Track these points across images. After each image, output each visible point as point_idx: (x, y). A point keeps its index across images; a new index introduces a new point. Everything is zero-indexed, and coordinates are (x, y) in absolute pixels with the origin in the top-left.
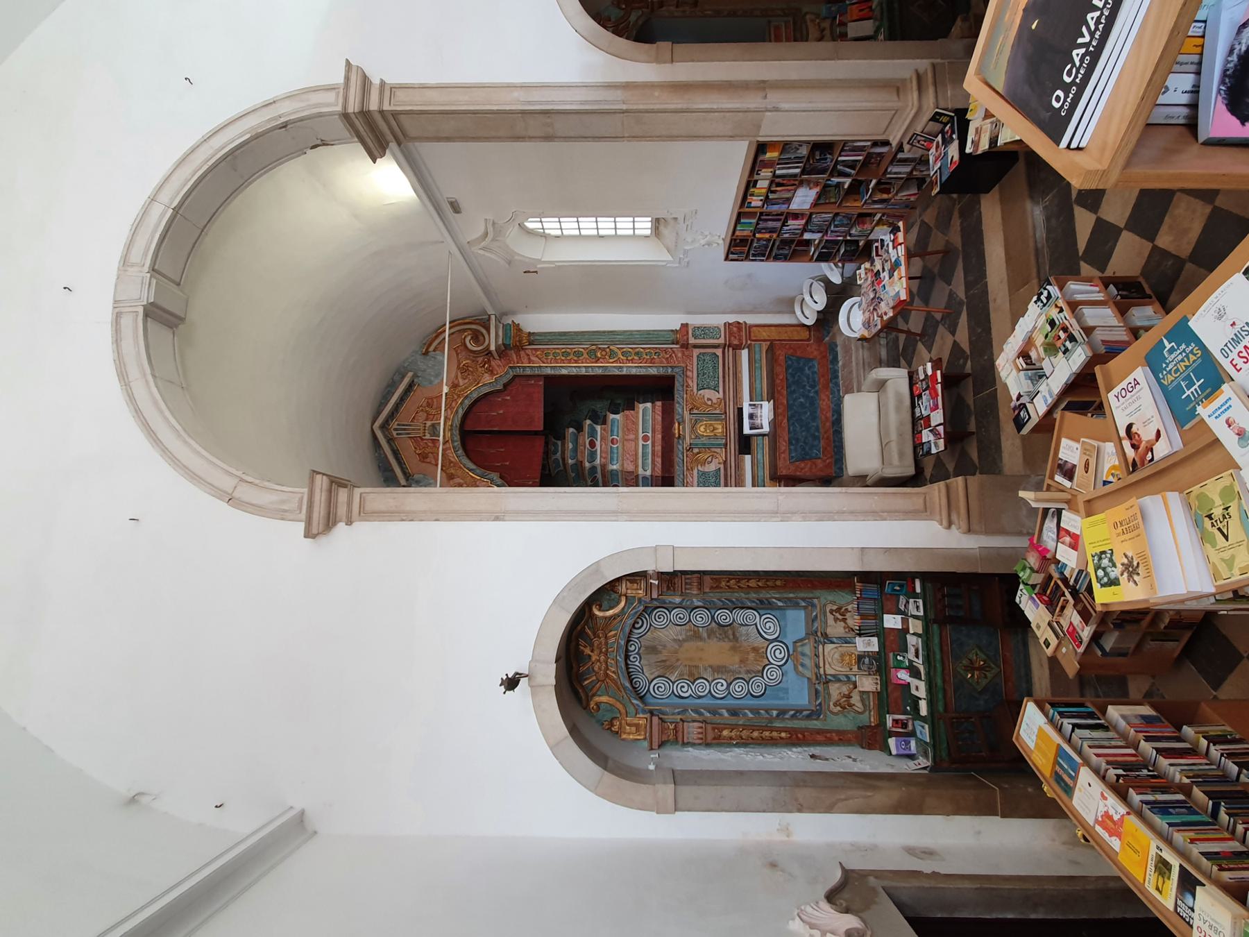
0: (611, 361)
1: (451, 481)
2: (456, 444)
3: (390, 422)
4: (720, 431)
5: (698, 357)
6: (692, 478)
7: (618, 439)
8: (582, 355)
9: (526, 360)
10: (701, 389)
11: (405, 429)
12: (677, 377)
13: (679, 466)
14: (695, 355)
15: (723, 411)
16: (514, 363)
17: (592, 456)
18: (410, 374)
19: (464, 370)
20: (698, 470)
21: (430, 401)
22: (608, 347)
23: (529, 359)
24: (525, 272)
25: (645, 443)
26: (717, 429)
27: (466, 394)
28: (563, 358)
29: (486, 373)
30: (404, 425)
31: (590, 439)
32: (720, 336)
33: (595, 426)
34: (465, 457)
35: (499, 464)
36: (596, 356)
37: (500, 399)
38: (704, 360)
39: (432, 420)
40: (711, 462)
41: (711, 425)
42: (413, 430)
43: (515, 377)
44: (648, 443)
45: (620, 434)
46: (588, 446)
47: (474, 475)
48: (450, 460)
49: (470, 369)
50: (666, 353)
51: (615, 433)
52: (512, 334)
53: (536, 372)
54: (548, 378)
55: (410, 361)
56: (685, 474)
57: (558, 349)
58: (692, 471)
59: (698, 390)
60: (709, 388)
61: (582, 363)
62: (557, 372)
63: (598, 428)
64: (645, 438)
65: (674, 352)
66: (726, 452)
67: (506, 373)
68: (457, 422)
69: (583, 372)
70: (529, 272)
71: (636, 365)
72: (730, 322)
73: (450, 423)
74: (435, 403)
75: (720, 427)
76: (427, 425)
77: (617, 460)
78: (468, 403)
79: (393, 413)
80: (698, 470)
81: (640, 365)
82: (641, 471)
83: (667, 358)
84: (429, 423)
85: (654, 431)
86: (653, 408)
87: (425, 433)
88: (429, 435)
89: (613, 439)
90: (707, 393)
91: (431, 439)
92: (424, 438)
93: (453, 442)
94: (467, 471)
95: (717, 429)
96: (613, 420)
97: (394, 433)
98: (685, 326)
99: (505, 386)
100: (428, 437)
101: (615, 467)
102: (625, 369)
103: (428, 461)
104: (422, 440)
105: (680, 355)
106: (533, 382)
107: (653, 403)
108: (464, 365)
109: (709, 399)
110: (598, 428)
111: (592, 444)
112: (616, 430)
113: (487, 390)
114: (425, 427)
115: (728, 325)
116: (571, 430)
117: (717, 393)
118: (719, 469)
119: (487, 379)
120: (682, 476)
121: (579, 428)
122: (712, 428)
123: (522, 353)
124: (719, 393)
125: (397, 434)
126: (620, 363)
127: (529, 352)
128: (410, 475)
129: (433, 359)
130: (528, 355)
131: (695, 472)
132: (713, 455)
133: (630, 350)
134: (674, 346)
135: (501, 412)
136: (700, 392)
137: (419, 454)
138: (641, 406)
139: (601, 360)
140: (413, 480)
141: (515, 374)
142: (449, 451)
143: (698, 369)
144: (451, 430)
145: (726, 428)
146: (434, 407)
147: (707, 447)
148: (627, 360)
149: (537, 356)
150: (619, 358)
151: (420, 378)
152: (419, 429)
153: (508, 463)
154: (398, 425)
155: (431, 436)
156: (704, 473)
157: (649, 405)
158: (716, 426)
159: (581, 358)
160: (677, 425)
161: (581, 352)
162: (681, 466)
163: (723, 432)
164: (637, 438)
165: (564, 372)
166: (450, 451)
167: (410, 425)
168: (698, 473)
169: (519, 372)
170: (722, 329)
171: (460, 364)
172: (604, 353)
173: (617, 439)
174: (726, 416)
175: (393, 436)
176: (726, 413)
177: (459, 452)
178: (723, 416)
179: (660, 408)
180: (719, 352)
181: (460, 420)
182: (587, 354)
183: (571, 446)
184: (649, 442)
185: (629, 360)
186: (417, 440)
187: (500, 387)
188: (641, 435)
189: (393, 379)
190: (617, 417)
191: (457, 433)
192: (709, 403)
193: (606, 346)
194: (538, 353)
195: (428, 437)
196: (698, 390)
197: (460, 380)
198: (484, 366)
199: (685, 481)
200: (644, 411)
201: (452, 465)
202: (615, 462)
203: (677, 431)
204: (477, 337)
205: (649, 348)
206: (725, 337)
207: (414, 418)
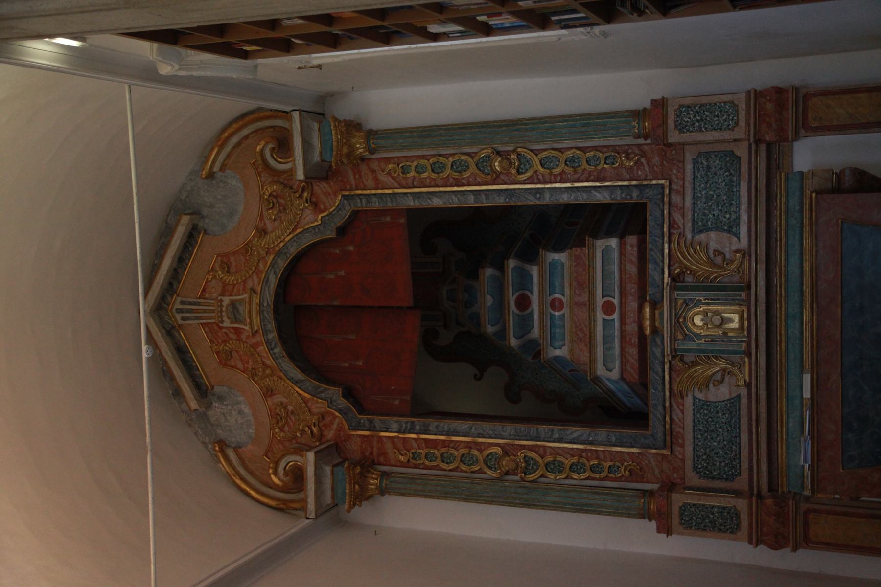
0: (522, 177)
1: (269, 399)
2: (270, 336)
3: (169, 298)
4: (735, 325)
5: (695, 161)
6: (683, 412)
7: (564, 300)
8: (468, 167)
9: (370, 182)
10: (701, 232)
11: (192, 311)
12: (650, 207)
13: (656, 389)
14: (689, 157)
15: (746, 277)
16: (351, 190)
17: (525, 324)
18: (185, 219)
19: (273, 202)
20: (694, 398)
21: (225, 260)
22: (514, 151)
23: (376, 179)
24: (299, 68)
25: (606, 317)
26: (731, 320)
27: (277, 249)
28: (434, 176)
29: (306, 208)
30: (191, 304)
31: (517, 294)
32: (737, 124)
33: (528, 267)
34: (287, 359)
35: (347, 365)
36: (493, 171)
37: (337, 252)
38: (709, 168)
39: (231, 295)
40: (721, 381)
41: (717, 313)
42: (205, 311)
43: (356, 214)
44: (611, 317)
45: (567, 291)
46: (513, 307)
47: (300, 392)
48: (264, 364)
49: (282, 201)
50: (628, 158)
51: (557, 290)
52: (335, 144)
53: (389, 204)
54: (412, 214)
55: (189, 189)
56: (667, 404)
57: (423, 157)
58: (682, 397)
59: (697, 231)
60: (718, 228)
61: (469, 185)
62: (425, 204)
63: (535, 271)
64: (608, 308)
65: (643, 154)
66: (750, 364)
67: (339, 209)
68: (269, 297)
69: (471, 202)
70: (305, 68)
71: (568, 185)
72: (758, 89)
73: (258, 301)
74: (234, 264)
75: (736, 317)
76: (225, 303)
77: (564, 340)
78: (282, 264)
79: (171, 284)
80: (694, 398)
81: (576, 185)
82: (601, 370)
83: (631, 167)
84: (226, 300)
85: (623, 294)
86: (622, 246)
87: (221, 316)
88: (229, 321)
89: (554, 300)
90: (713, 239)
91: (234, 328)
92: (221, 325)
93: (266, 332)
94: (291, 384)
95: (731, 320)
96: (553, 264)
97: (178, 317)
98: (660, 104)
99: (342, 231)
100: (227, 323)
101: (558, 352)
102: (547, 196)
103: (233, 364)
104: (221, 328)
105: (656, 160)
106: (388, 219)
107: (622, 237)
108: (270, 195)
109: (717, 253)
110: (535, 271)
111: (523, 303)
112: (557, 284)
113: (308, 240)
114: (221, 306)
115: (757, 96)
116: (489, 272)
117: (735, 239)
118: (739, 396)
119: (311, 219)
120: (660, 408)
121: (501, 268)
122: (717, 320)
123: (364, 168)
124: (739, 238)
125: (183, 319)
126: (540, 182)
127: (375, 165)
128: (207, 389)
129: (222, 185)
130: (373, 171)
131: (688, 401)
132: (724, 370)
133: (555, 153)
134: (641, 141)
135: (342, 273)
136: (697, 237)
137: (217, 353)
138: (600, 244)
139: (502, 177)
140: (214, 395)
141: (353, 208)
142: (261, 348)
143: (694, 188)
144: (260, 312)
145: (748, 319)
146: (233, 270)
147: (708, 356)
148: (551, 174)
149: (389, 174)
150: (536, 172)
151: (207, 220)
152: (213, 311)
153: (360, 364)
154: (182, 303)
155: (231, 323)
156: (707, 404)
157: (614, 242)
158: (726, 315)
159: (466, 175)
160: (647, 310)
161: (466, 162)
162: (660, 388)
163: (741, 327)
164: (592, 309)
165: (437, 202)
166: (262, 348)
167: (199, 304)
168: (694, 404)
169: (361, 205)
170: (742, 106)
171: (264, 193)
172: (505, 164)
173: (561, 301)
174: (749, 295)
175: (176, 321)
176: (749, 287)
177: (276, 351)
178: (743, 295)
179: (635, 249)
180: (741, 151)
181: (273, 293)
182: (477, 165)
183: (489, 300)
184: (615, 316)
185: (555, 176)
186: (213, 329)
187: (331, 234)
188: (600, 301)
189: (167, 222)
190: (556, 256)
191: (269, 316)
192: (719, 260)
193: (511, 149)
194: (390, 166)
195: (227, 323)
196: (697, 231)
197: (268, 222)
198: (301, 196)
199: (667, 419)
200: (606, 253)
201: (268, 371)
202: (557, 344)
203: (648, 323)
204: (283, 145)
205: (595, 148)
206: (748, 124)
207: (204, 290)
